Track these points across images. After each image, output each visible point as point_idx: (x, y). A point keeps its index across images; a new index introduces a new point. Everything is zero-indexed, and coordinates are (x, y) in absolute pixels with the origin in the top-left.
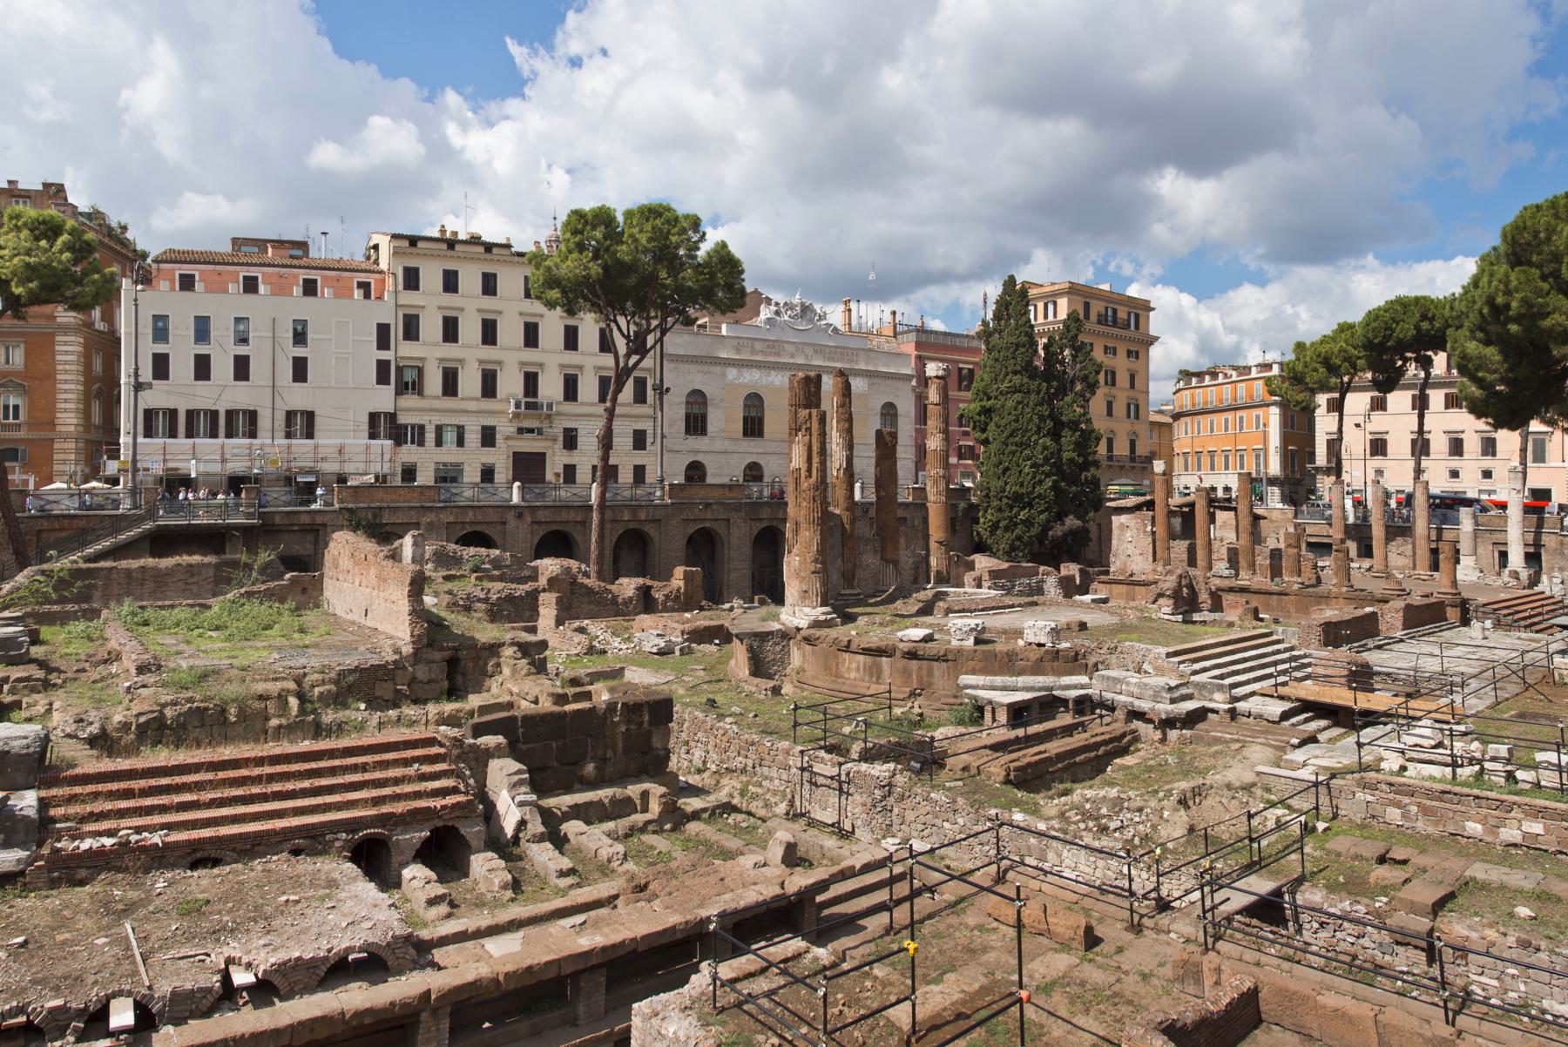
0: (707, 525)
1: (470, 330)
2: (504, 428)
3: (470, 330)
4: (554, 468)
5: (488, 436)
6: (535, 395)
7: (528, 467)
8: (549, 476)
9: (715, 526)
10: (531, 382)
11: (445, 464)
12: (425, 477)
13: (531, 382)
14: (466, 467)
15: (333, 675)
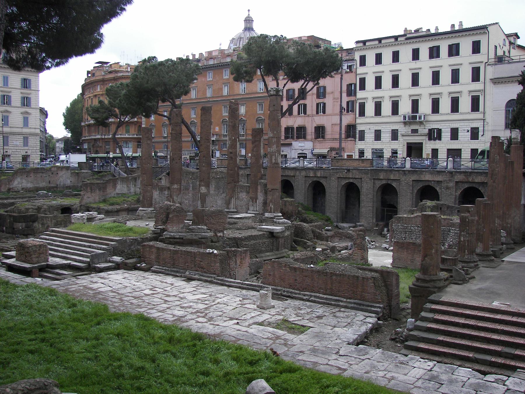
0: (351, 181)
1: (445, 77)
2: (402, 129)
3: (387, 82)
4: (427, 150)
5: (395, 135)
6: (417, 112)
7: (414, 150)
8: (424, 156)
9: (355, 181)
10: (415, 104)
11: (376, 150)
12: (368, 155)
13: (415, 104)
14: (384, 151)
15: (36, 207)
